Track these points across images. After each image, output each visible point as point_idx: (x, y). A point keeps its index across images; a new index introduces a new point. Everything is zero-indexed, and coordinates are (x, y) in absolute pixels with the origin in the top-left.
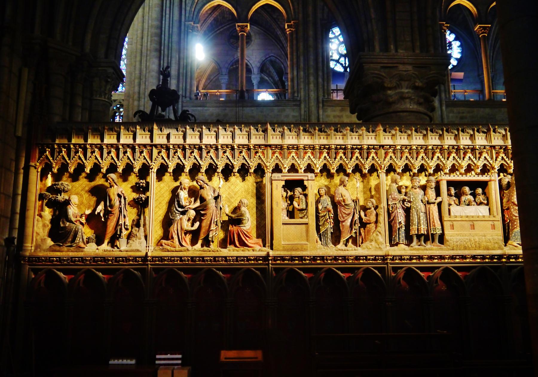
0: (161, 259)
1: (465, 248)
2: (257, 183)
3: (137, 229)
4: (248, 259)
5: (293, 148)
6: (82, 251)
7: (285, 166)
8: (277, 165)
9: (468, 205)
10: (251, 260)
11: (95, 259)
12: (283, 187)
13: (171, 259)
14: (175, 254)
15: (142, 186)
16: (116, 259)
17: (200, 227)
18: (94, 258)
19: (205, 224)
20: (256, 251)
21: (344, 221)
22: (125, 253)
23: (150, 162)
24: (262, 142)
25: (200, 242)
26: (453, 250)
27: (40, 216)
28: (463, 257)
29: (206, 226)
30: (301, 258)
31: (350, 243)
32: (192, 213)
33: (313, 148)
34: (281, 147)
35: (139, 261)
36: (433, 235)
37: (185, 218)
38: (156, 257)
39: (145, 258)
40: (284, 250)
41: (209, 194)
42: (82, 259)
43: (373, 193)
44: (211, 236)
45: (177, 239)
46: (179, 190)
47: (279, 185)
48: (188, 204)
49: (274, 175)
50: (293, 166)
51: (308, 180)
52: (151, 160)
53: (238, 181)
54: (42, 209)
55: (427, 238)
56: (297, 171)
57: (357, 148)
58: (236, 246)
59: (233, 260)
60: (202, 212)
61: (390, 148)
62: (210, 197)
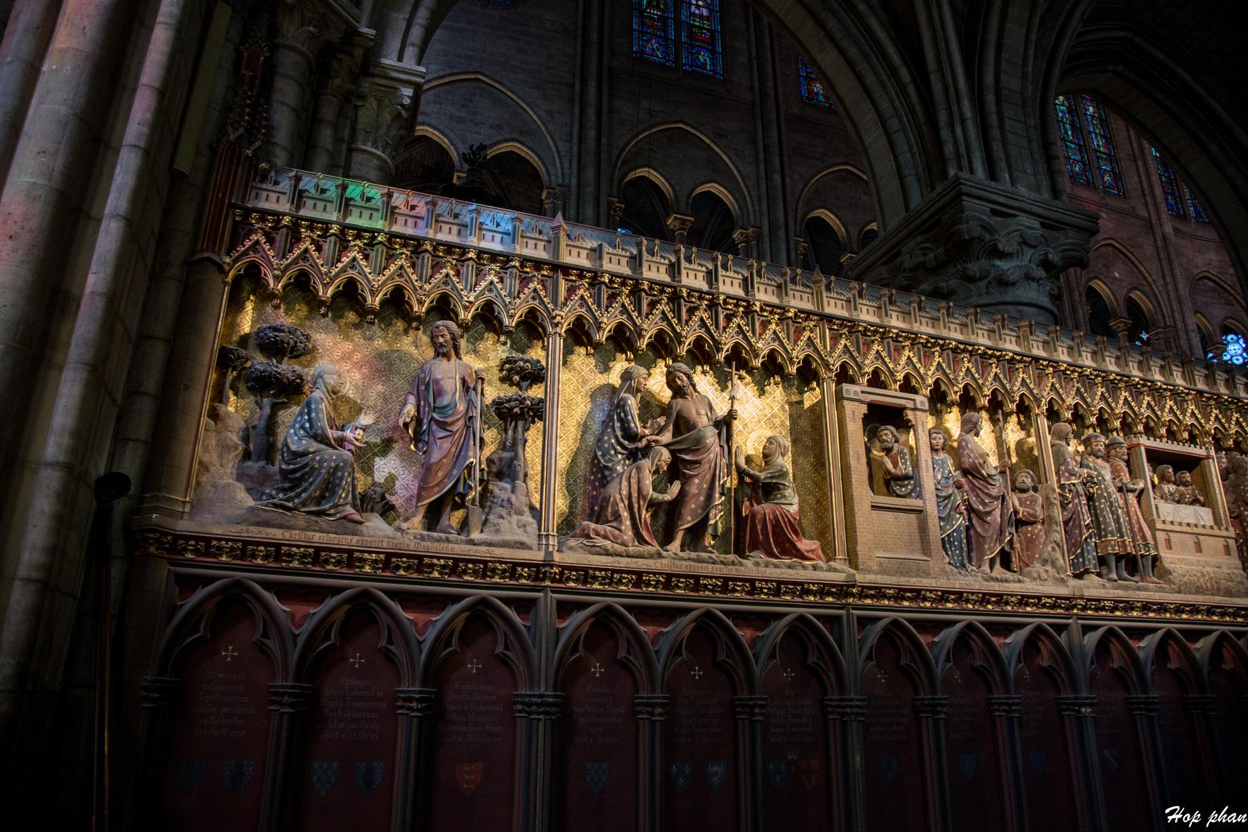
0: (585, 574)
1: (1199, 590)
2: (791, 404)
3: (508, 486)
4: (802, 588)
5: (875, 332)
6: (354, 534)
7: (867, 370)
8: (844, 366)
9: (1178, 502)
10: (809, 592)
11: (389, 560)
12: (867, 420)
13: (612, 575)
14: (624, 563)
15: (522, 369)
16: (456, 566)
17: (682, 493)
18: (389, 556)
19: (697, 486)
20: (821, 569)
21: (989, 513)
22: (484, 549)
23: (550, 306)
24: (809, 306)
25: (679, 536)
26: (1179, 592)
27: (214, 415)
28: (1195, 609)
29: (699, 494)
30: (918, 594)
31: (997, 566)
32: (666, 455)
33: (914, 338)
34: (851, 325)
35: (521, 576)
36: (1142, 556)
37: (646, 464)
38: (571, 568)
39: (538, 571)
40: (883, 571)
41: (703, 412)
42: (351, 558)
43: (1014, 460)
44: (712, 522)
45: (628, 523)
46: (622, 394)
47: (855, 413)
48: (647, 432)
49: (845, 386)
50: (876, 372)
51: (915, 409)
52: (556, 304)
53: (750, 394)
54: (219, 397)
55: (1131, 564)
56: (883, 385)
57: (992, 356)
58: (770, 554)
59: (769, 589)
60: (687, 457)
61: (1047, 366)
62: (705, 420)
